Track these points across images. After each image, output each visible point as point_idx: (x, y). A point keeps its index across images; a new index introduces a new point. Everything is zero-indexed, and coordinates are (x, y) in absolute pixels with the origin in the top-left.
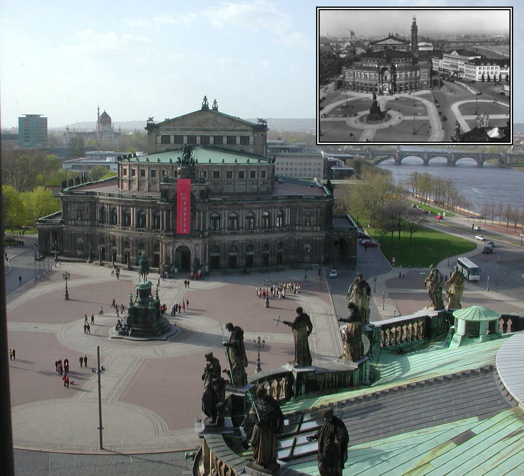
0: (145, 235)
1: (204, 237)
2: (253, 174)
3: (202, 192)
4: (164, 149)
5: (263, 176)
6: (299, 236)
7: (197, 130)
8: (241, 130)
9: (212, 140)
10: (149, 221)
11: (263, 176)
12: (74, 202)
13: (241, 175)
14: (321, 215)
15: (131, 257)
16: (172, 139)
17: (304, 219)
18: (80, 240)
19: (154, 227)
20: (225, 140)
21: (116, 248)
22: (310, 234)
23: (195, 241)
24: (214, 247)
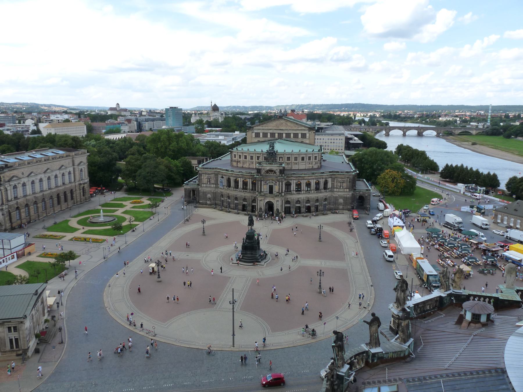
0: (248, 195)
1: (281, 196)
2: (310, 158)
3: (280, 170)
4: (256, 140)
5: (316, 159)
6: (336, 194)
7: (275, 130)
8: (301, 130)
9: (284, 135)
10: (250, 186)
11: (316, 159)
12: (206, 174)
13: (303, 159)
14: (349, 182)
15: (239, 206)
16: (261, 135)
17: (339, 185)
18: (209, 196)
19: (252, 190)
20: (292, 135)
21: (229, 200)
22: (342, 194)
23: (276, 199)
24: (288, 202)
